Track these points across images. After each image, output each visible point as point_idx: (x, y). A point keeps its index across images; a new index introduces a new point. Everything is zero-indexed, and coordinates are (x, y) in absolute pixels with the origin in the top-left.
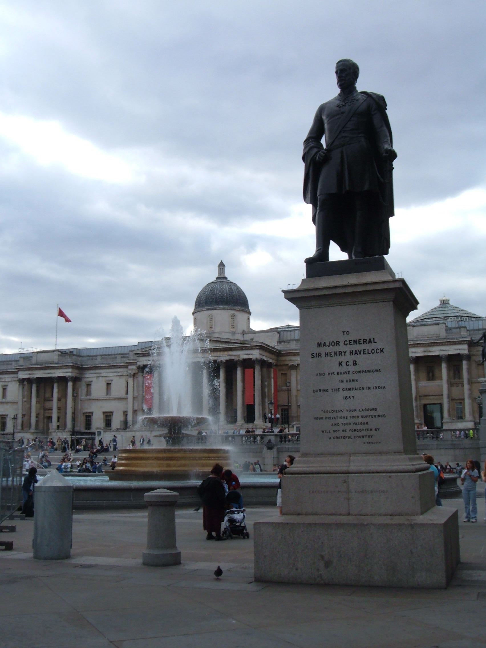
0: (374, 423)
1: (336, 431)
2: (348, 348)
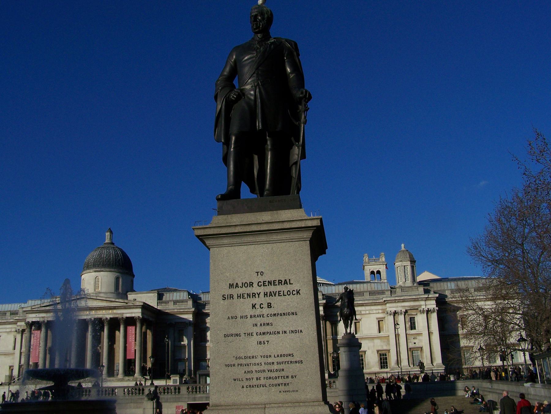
1: (250, 379)
2: (262, 290)
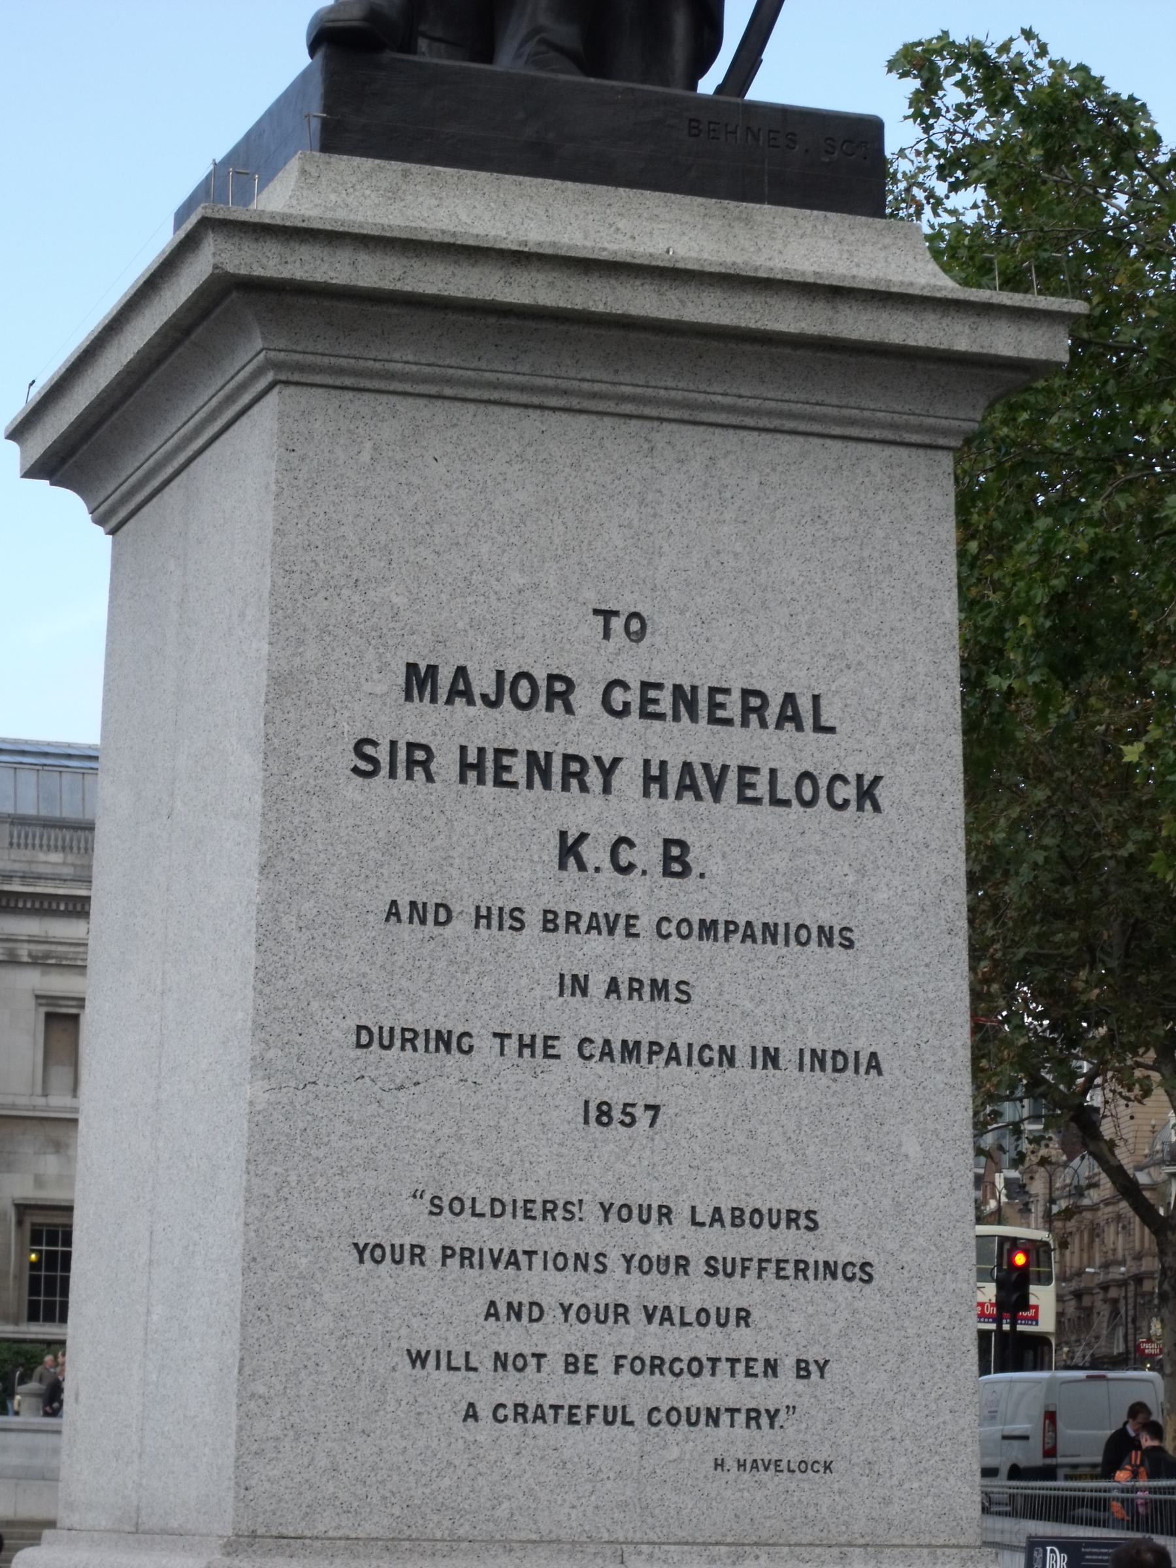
0: (788, 1318)
1: (519, 1363)
2: (633, 742)
